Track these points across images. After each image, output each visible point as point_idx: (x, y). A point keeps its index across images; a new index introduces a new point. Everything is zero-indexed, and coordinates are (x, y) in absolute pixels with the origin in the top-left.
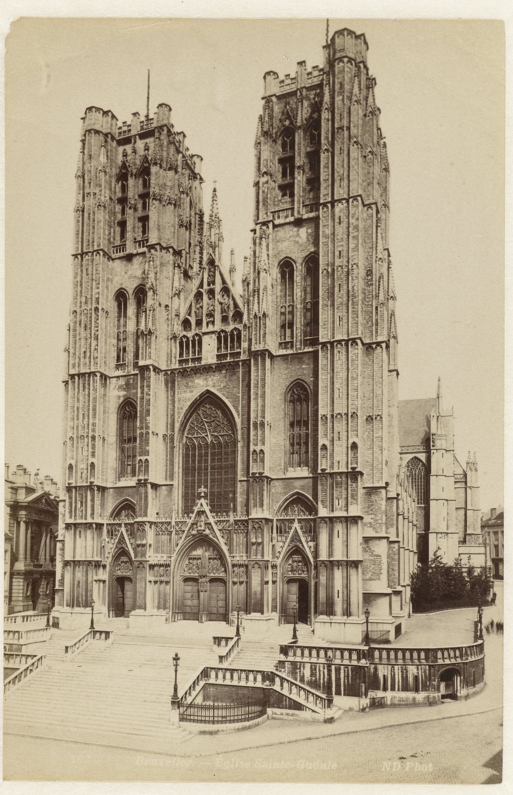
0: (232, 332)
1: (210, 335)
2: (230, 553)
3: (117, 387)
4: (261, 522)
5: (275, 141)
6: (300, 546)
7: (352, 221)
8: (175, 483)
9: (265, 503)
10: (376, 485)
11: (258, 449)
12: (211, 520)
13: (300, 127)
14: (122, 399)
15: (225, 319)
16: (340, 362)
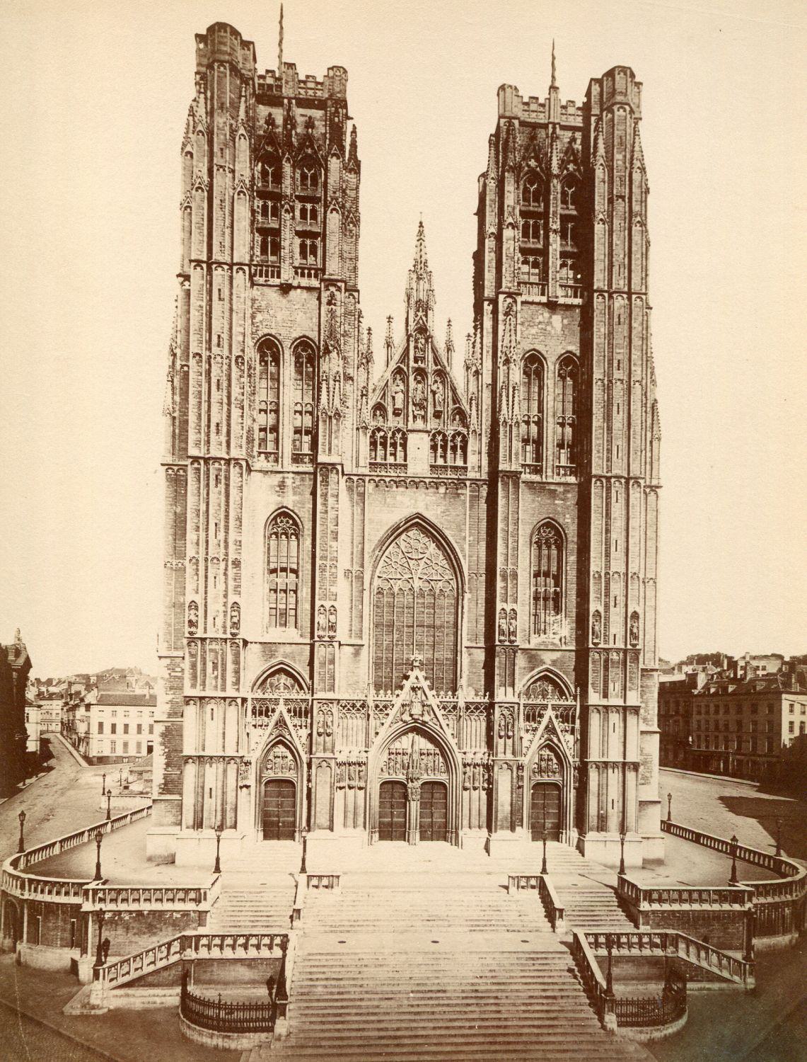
6: (555, 740)
11: (508, 607)
12: (433, 701)
13: (557, 176)
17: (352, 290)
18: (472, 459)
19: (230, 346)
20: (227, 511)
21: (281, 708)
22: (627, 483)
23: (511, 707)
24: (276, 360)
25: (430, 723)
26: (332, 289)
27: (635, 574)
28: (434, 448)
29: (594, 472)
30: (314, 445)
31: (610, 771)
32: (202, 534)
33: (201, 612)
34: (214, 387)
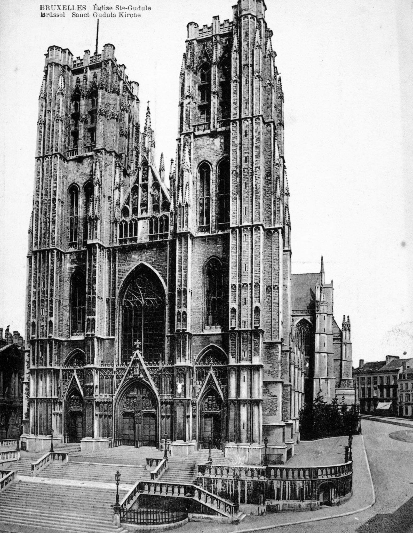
0: (161, 217)
1: (144, 220)
2: (160, 394)
4: (184, 369)
5: (195, 73)
7: (255, 134)
8: (116, 338)
9: (187, 353)
10: (274, 341)
12: (145, 367)
13: (215, 63)
15: (156, 209)
16: (246, 243)
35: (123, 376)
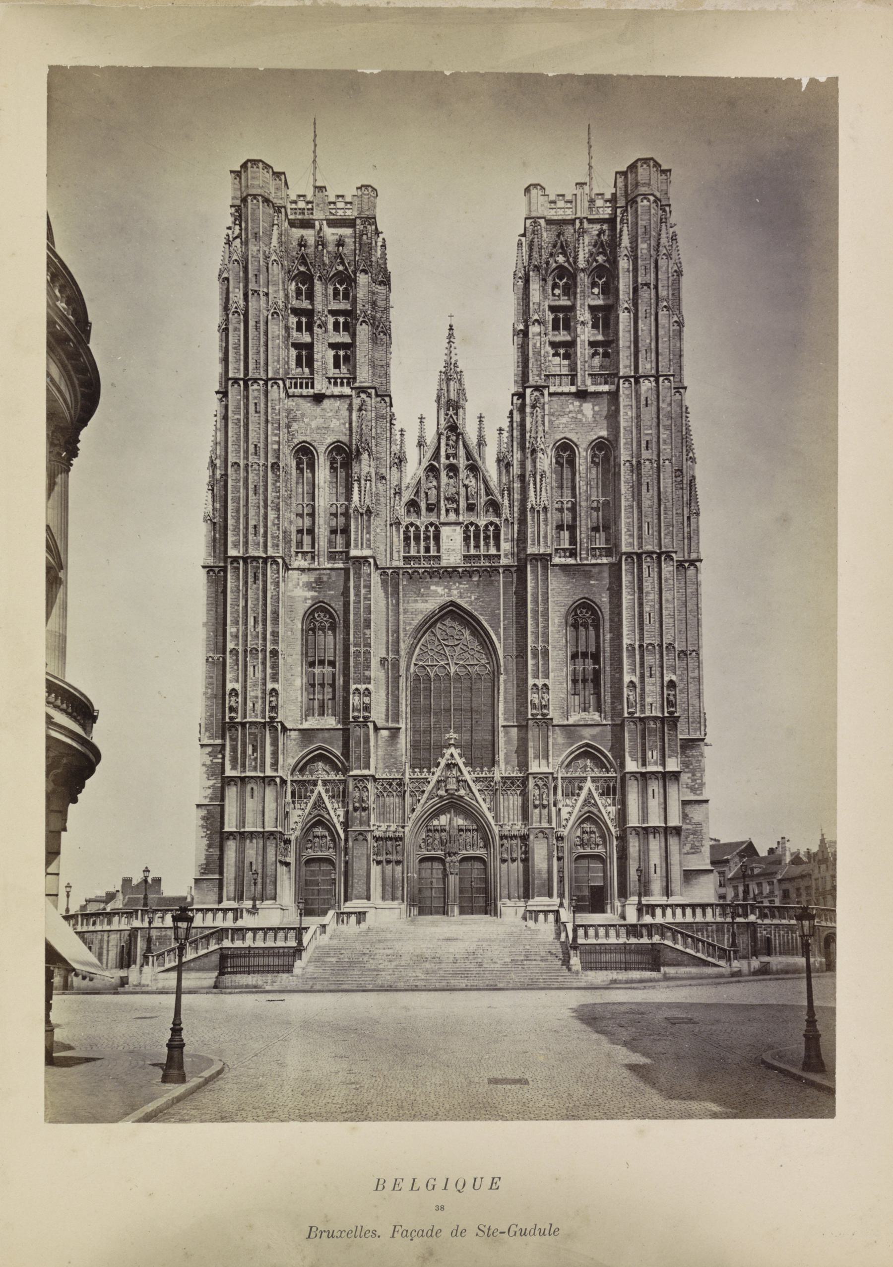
0: (486, 526)
1: (453, 527)
3: (301, 584)
4: (547, 777)
5: (544, 280)
6: (595, 811)
8: (402, 725)
9: (550, 753)
12: (468, 777)
13: (583, 270)
14: (309, 603)
17: (385, 396)
18: (505, 546)
19: (266, 454)
20: (265, 605)
21: (320, 788)
22: (659, 558)
23: (544, 777)
24: (312, 466)
25: (466, 798)
26: (363, 396)
27: (670, 644)
28: (466, 539)
29: (624, 549)
30: (348, 545)
31: (651, 836)
32: (241, 628)
33: (240, 700)
34: (251, 493)
35: (423, 792)
